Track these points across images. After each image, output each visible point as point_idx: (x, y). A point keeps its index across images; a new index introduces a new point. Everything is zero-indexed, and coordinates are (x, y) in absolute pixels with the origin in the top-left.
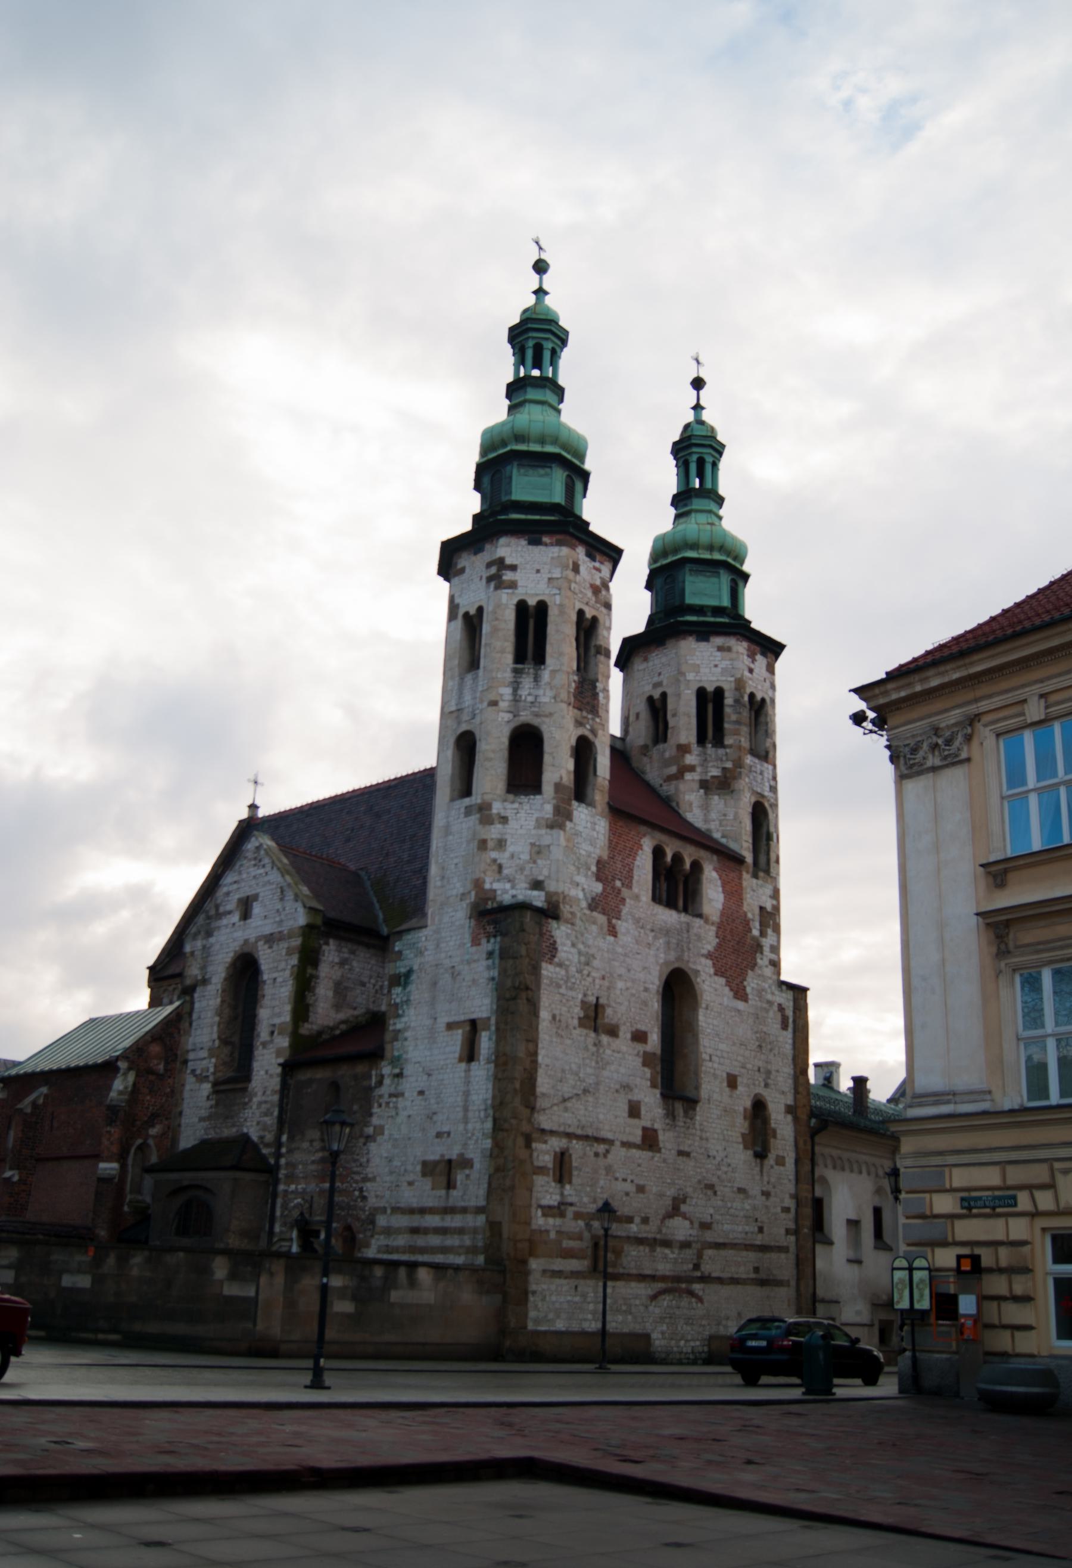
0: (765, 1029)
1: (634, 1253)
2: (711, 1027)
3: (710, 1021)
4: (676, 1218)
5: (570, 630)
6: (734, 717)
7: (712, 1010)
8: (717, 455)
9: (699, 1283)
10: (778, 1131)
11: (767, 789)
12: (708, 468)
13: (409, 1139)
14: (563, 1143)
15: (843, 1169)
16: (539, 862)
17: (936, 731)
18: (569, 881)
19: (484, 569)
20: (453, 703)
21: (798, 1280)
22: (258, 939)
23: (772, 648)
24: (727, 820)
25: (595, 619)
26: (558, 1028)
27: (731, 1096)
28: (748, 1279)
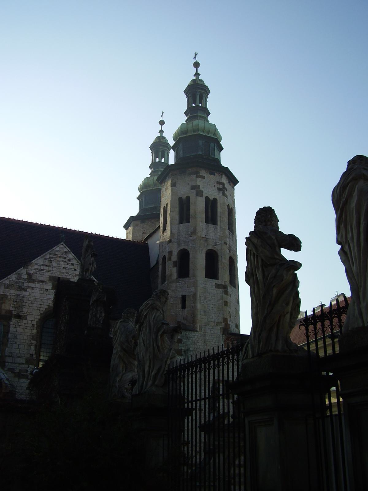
19: (216, 183)
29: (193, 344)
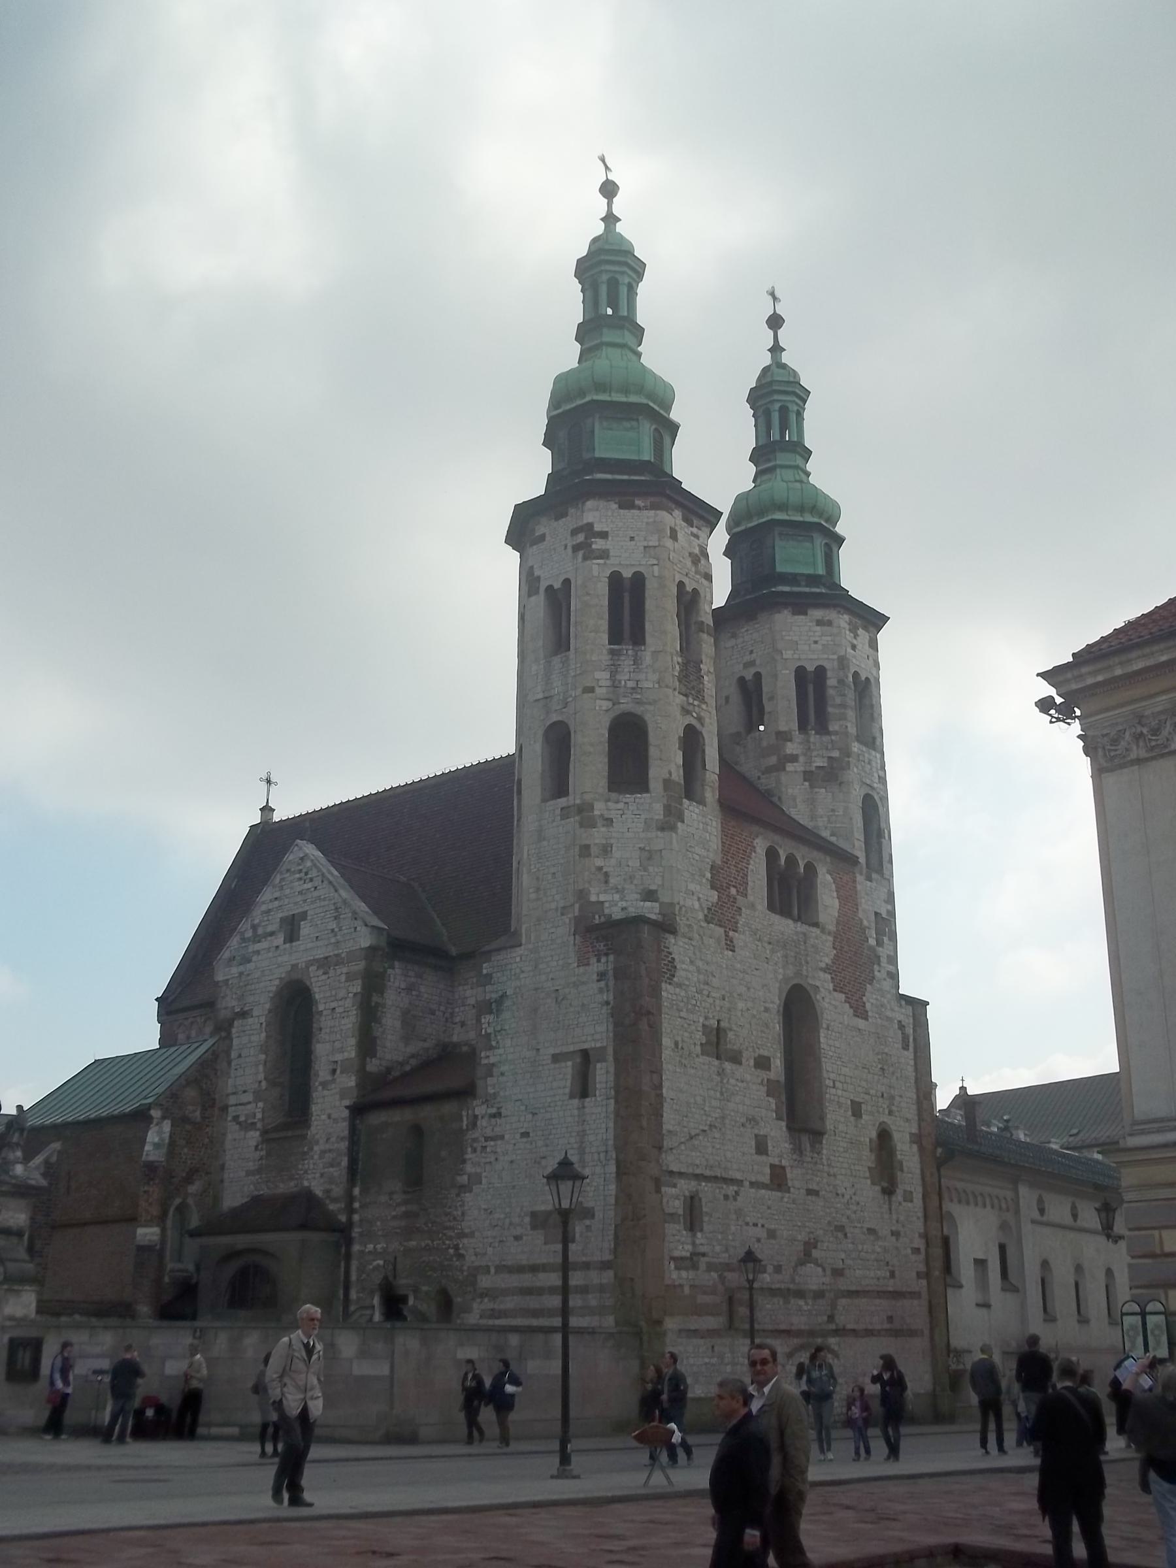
0: (886, 1050)
1: (768, 1306)
2: (833, 1049)
3: (831, 1042)
4: (809, 1265)
5: (672, 605)
6: (838, 700)
7: (833, 1031)
8: (801, 403)
9: (834, 1337)
10: (905, 1164)
11: (877, 780)
12: (793, 417)
13: (514, 1187)
14: (693, 1183)
15: (968, 1203)
16: (651, 869)
17: (1140, 719)
18: (684, 890)
19: (569, 537)
20: (539, 688)
21: (932, 1329)
22: (310, 963)
23: (874, 620)
24: (837, 816)
25: (695, 592)
26: (681, 1056)
27: (856, 1126)
28: (882, 1330)
29: (513, 977)
